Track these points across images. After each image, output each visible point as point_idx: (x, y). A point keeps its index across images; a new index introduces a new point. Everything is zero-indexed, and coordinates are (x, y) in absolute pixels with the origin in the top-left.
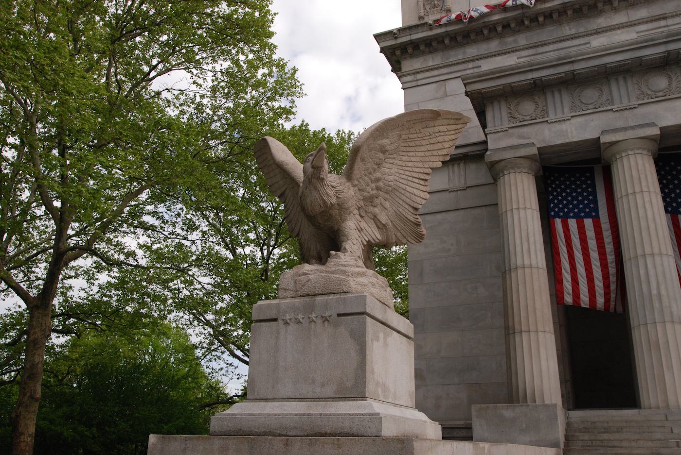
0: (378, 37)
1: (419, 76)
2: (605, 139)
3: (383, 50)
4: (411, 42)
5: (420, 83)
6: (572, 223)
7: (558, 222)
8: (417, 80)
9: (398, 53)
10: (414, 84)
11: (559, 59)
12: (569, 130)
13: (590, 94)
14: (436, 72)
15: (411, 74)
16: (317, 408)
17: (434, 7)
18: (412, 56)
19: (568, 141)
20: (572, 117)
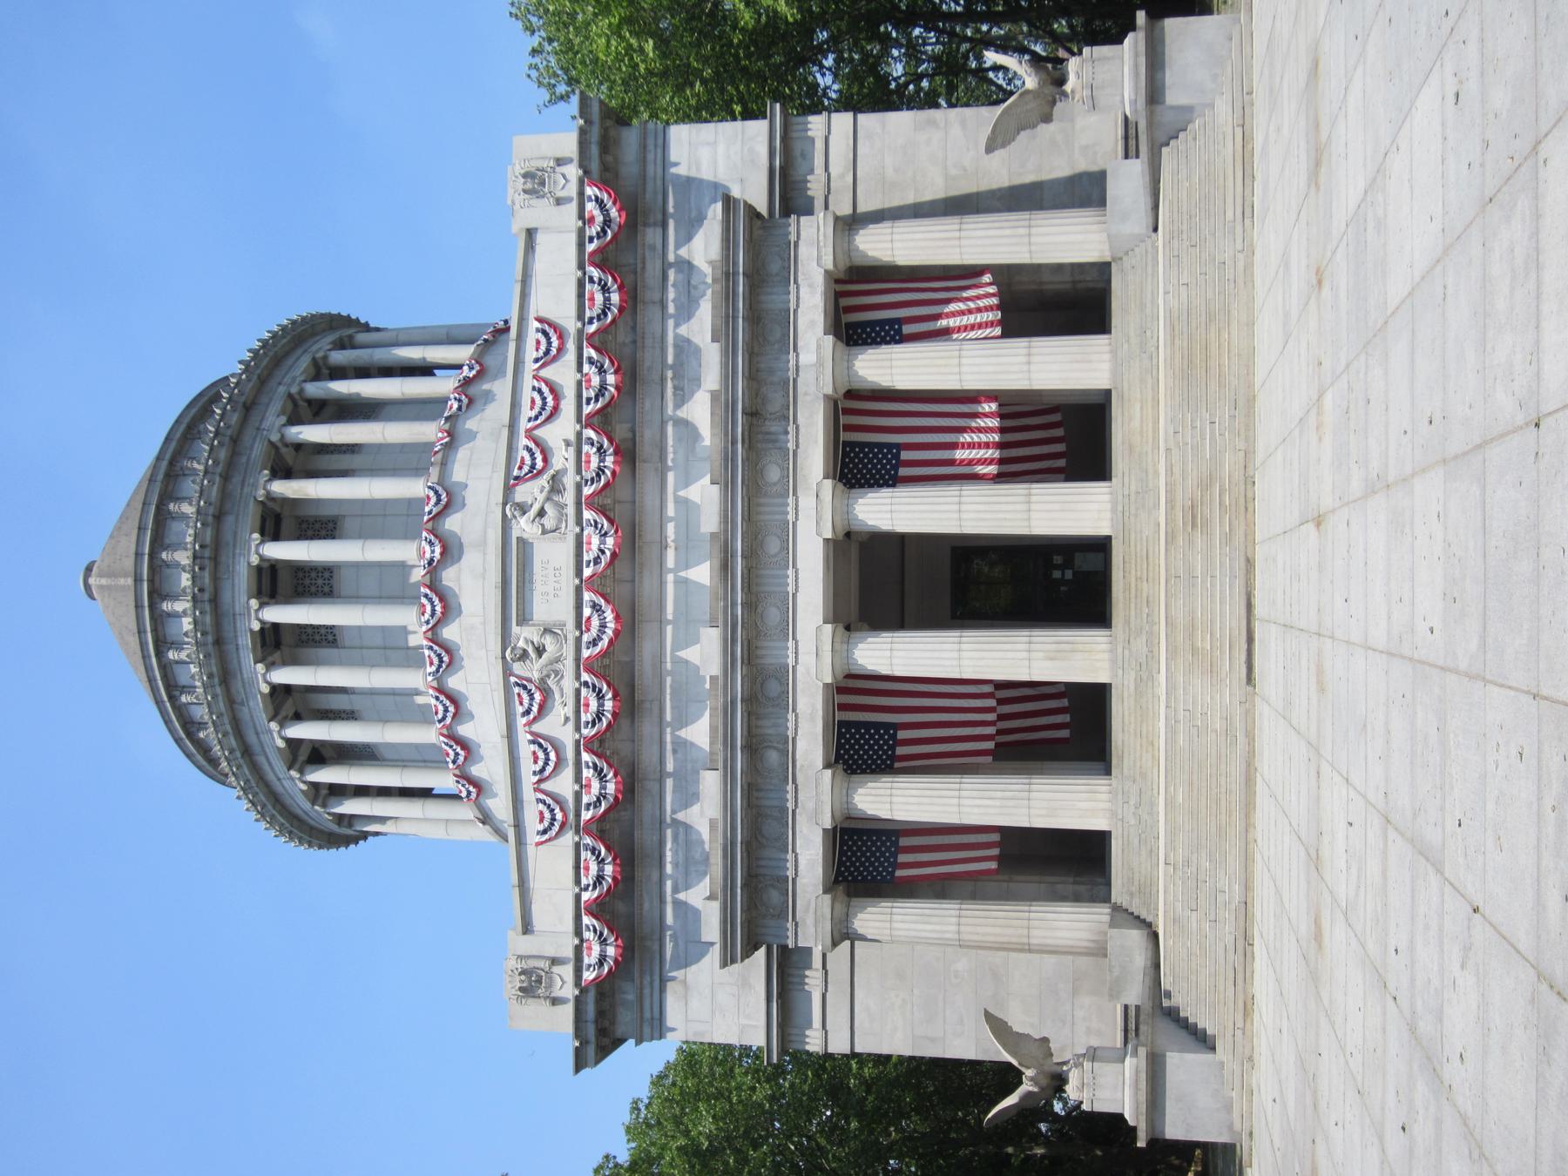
0: (579, 1066)
1: (647, 1015)
2: (828, 825)
3: (597, 1062)
4: (596, 1022)
5: (656, 1014)
6: (902, 858)
7: (899, 873)
8: (652, 1019)
9: (606, 1041)
10: (656, 1023)
11: (725, 857)
12: (808, 857)
13: (770, 828)
14: (647, 991)
15: (641, 1027)
16: (1127, 1082)
17: (539, 981)
18: (613, 1023)
19: (821, 860)
20: (793, 851)
